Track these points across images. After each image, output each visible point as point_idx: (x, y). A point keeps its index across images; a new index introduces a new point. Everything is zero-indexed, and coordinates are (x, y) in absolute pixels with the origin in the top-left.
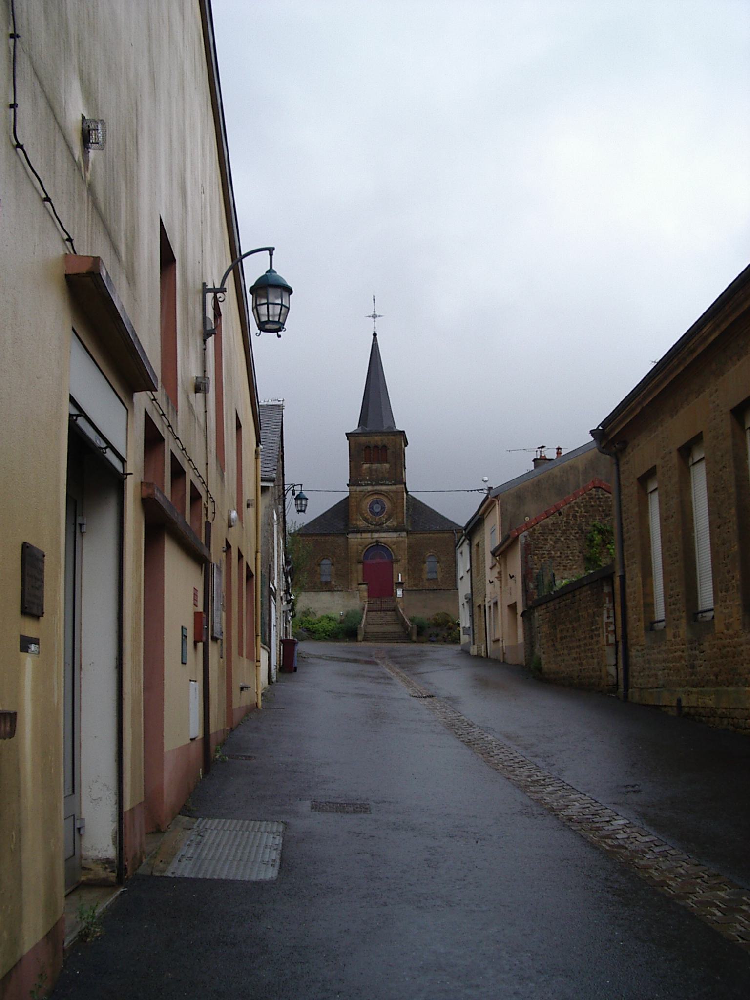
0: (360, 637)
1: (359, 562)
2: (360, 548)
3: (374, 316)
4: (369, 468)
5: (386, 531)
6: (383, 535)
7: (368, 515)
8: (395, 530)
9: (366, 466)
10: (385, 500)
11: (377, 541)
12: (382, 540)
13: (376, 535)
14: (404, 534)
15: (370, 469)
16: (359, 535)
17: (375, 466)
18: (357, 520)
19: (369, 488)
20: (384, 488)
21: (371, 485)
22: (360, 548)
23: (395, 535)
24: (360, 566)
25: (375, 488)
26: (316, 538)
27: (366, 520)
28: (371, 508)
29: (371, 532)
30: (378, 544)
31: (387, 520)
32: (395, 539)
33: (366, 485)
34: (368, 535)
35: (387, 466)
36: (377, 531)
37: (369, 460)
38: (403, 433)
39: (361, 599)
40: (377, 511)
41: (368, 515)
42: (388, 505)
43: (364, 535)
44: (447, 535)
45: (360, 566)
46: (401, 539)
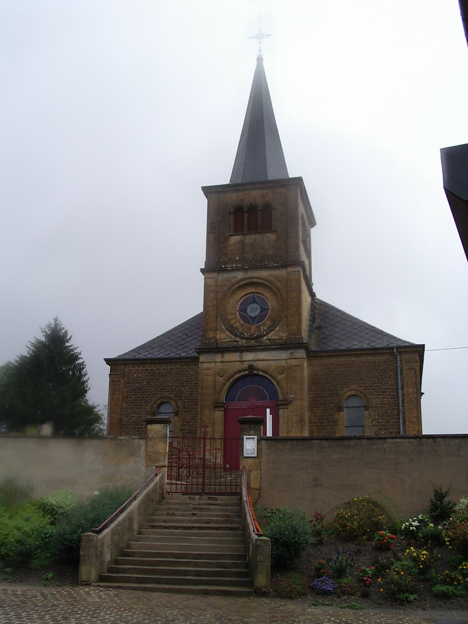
0: (88, 571)
1: (217, 406)
2: (220, 379)
3: (260, 37)
4: (242, 241)
5: (266, 348)
6: (262, 355)
7: (237, 322)
8: (283, 346)
9: (235, 239)
10: (268, 295)
11: (251, 368)
12: (260, 365)
13: (249, 356)
14: (301, 353)
15: (242, 243)
16: (218, 358)
17: (249, 239)
18: (216, 329)
19: (240, 275)
20: (264, 274)
21: (242, 269)
22: (220, 379)
23: (283, 355)
24: (219, 414)
25: (251, 274)
26: (150, 367)
27: (232, 330)
28: (243, 310)
29: (241, 350)
30: (252, 374)
31: (270, 329)
32: (283, 363)
33: (233, 270)
34: (235, 357)
35: (272, 237)
36: (250, 349)
37: (238, 230)
38: (299, 181)
39: (151, 458)
40: (253, 315)
41: (237, 322)
42: (272, 302)
43: (229, 357)
44: (381, 358)
45: (219, 414)
46: (294, 362)
